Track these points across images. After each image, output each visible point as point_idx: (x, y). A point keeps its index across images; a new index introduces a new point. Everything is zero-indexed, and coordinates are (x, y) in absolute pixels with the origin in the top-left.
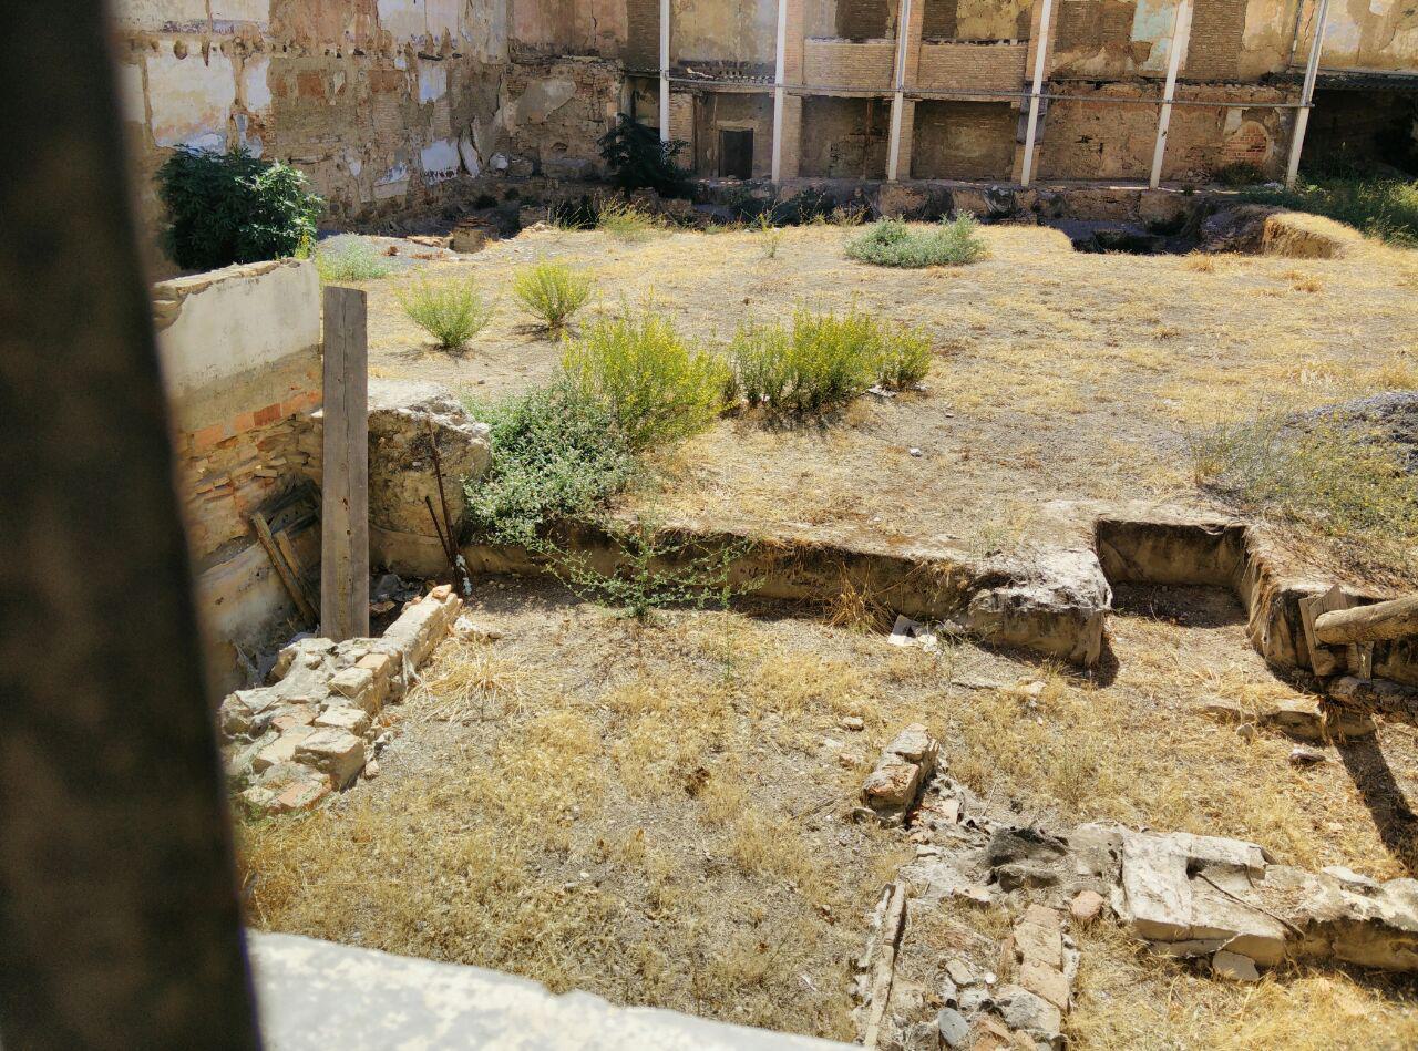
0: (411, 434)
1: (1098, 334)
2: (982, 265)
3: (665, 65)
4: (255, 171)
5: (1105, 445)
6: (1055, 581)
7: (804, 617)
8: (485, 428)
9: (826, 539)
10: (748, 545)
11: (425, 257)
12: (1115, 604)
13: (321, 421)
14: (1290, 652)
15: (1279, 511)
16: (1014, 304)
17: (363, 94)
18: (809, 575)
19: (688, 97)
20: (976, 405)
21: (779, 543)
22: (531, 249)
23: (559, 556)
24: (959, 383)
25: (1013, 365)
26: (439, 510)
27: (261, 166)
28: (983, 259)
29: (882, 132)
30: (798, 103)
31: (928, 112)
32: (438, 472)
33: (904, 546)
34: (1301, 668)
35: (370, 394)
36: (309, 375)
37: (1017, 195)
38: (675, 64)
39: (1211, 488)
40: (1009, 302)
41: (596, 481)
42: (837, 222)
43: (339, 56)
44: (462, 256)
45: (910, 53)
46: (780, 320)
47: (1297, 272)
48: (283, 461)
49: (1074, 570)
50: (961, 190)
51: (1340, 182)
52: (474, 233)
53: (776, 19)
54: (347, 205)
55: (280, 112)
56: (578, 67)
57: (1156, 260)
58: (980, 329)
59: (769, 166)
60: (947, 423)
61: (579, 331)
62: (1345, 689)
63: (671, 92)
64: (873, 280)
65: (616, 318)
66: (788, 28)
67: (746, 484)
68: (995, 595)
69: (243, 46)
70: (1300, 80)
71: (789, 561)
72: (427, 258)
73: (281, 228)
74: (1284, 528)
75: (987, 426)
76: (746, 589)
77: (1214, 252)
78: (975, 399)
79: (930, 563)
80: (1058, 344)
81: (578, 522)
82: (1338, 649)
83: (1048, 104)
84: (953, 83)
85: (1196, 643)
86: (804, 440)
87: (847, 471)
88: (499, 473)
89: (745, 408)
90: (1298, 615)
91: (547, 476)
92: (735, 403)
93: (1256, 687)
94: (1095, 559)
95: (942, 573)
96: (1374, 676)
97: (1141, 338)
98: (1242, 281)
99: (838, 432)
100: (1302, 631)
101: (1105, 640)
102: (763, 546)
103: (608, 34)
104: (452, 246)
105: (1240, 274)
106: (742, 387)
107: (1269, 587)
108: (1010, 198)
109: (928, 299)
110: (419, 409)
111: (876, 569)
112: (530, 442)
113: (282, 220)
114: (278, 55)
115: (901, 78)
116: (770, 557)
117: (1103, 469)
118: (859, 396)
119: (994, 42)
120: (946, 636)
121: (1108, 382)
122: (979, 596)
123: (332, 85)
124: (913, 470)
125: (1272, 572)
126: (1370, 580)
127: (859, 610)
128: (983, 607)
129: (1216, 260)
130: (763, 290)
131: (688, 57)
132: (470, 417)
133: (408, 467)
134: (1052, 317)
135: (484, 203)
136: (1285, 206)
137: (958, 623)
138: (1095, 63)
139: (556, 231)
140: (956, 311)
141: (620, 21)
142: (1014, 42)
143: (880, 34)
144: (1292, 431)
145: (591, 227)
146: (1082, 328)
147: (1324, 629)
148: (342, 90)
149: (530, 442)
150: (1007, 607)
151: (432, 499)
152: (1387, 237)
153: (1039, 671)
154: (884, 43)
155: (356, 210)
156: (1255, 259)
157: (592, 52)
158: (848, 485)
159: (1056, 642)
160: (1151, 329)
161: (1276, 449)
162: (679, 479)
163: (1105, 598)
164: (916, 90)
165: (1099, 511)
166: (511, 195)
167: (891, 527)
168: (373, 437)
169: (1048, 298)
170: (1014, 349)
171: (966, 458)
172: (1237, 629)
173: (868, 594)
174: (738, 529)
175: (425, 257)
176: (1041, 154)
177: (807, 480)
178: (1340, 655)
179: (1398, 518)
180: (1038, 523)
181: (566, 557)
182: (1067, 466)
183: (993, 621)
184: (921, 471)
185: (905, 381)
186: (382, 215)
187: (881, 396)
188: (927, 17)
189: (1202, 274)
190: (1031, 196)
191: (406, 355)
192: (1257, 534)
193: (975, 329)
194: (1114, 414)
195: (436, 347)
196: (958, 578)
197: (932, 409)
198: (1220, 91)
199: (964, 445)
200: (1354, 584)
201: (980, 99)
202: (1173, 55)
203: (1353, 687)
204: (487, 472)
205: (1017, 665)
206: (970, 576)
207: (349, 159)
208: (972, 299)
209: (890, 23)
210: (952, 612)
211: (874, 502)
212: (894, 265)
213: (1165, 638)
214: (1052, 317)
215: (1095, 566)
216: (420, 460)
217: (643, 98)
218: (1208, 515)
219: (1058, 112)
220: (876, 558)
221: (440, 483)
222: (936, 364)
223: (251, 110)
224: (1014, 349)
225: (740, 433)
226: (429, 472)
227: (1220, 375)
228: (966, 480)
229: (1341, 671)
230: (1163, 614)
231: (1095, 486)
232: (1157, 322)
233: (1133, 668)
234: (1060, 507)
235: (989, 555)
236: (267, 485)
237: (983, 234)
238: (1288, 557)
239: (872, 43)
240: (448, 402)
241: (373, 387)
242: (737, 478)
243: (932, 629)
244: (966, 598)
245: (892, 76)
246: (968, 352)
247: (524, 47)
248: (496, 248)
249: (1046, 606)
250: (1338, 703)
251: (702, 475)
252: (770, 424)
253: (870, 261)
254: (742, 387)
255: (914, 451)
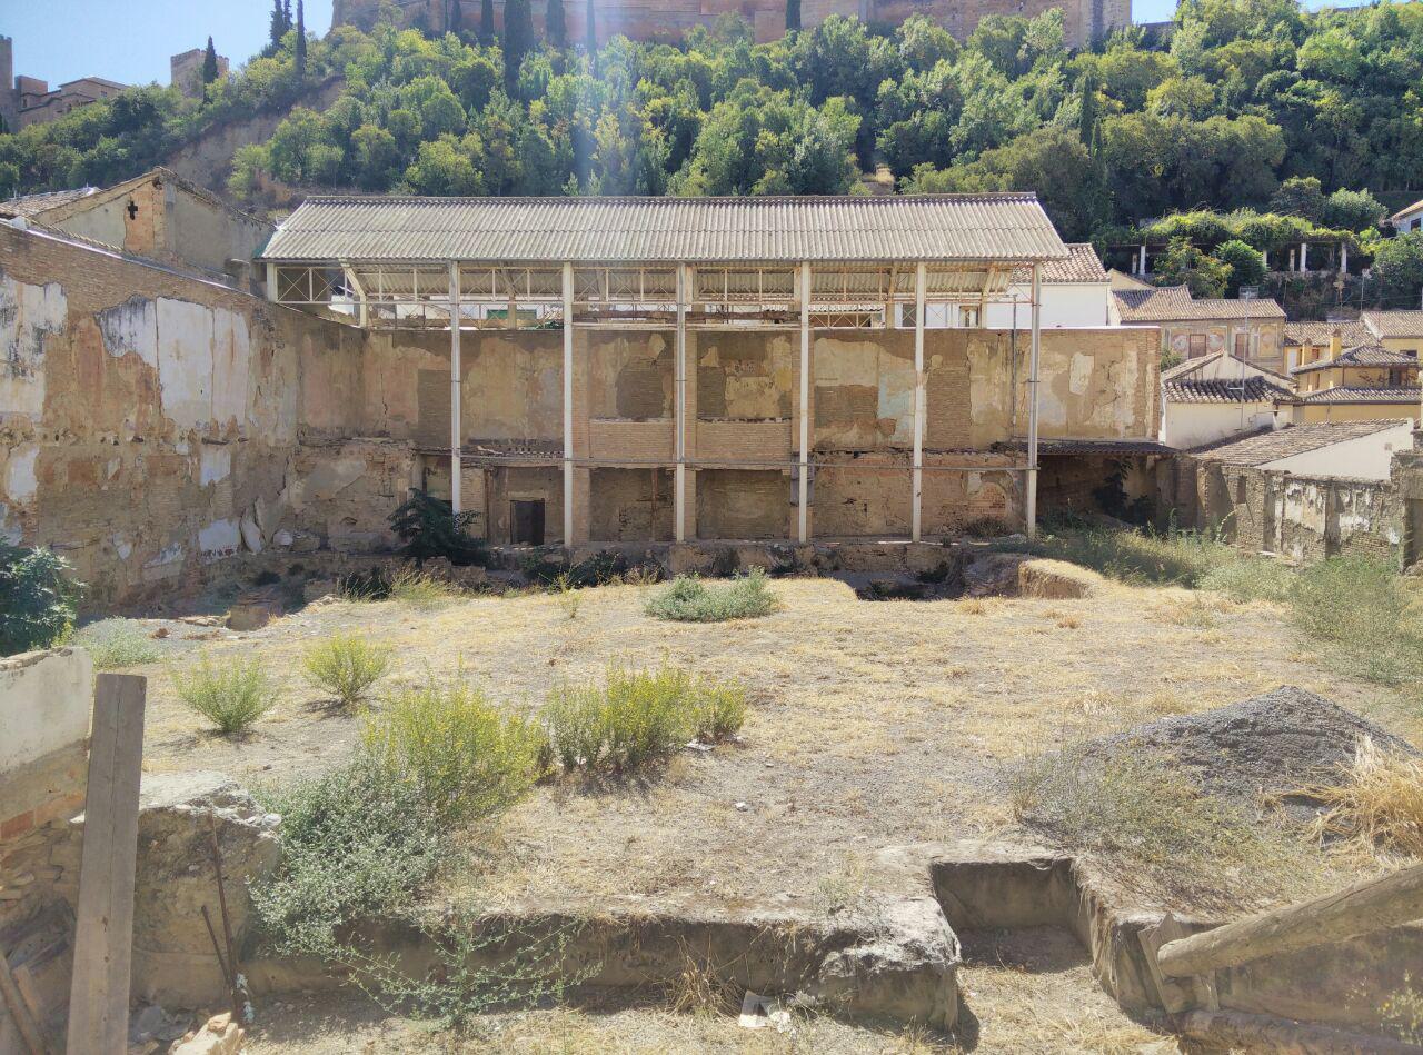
0: (189, 833)
1: (895, 675)
2: (776, 616)
3: (456, 443)
4: (11, 559)
5: (924, 786)
6: (903, 935)
7: (644, 1005)
8: (276, 818)
9: (662, 911)
10: (578, 926)
11: (198, 638)
12: (964, 955)
13: (81, 826)
14: (1140, 990)
15: (1099, 841)
16: (814, 652)
17: (140, 478)
18: (645, 954)
19: (480, 472)
20: (795, 753)
21: (612, 920)
22: (319, 622)
23: (362, 963)
24: (774, 732)
25: (823, 710)
26: (217, 920)
27: (18, 554)
28: (777, 610)
29: (667, 497)
30: (586, 474)
31: (709, 479)
32: (219, 875)
33: (744, 910)
34: (1152, 1006)
35: (142, 791)
36: (72, 775)
37: (797, 552)
38: (466, 443)
39: (1031, 822)
40: (808, 649)
41: (404, 869)
42: (633, 581)
43: (116, 443)
44: (242, 634)
45: (688, 429)
46: (590, 679)
47: (1057, 611)
48: (31, 878)
49: (919, 921)
50: (745, 547)
51: (1072, 531)
52: (254, 610)
53: (562, 401)
54: (112, 589)
55: (49, 501)
56: (369, 448)
57: (933, 605)
58: (785, 677)
59: (562, 532)
60: (768, 773)
61: (378, 704)
62: (1200, 1025)
63: (462, 467)
64: (676, 635)
65: (416, 688)
66: (574, 409)
67: (571, 858)
68: (845, 958)
69: (10, 435)
70: (1024, 448)
71: (624, 940)
72: (202, 638)
73: (35, 617)
74: (1107, 858)
75: (808, 774)
76: (580, 977)
77: (982, 596)
78: (792, 747)
79: (774, 926)
80: (860, 687)
81: (383, 918)
82: (1183, 982)
83: (815, 471)
84: (729, 455)
85: (1048, 991)
86: (626, 802)
87: (675, 831)
88: (290, 870)
89: (561, 774)
90: (1139, 949)
91: (347, 867)
92: (552, 769)
93: (1115, 1033)
94: (937, 907)
95: (787, 936)
96: (1222, 1007)
97: (935, 678)
98: (1011, 621)
99: (661, 791)
100: (1147, 966)
101: (960, 997)
102: (594, 925)
103: (397, 417)
104: (229, 624)
105: (1009, 614)
106: (557, 751)
107: (1107, 922)
108: (791, 553)
109: (732, 650)
110: (199, 803)
111: (718, 940)
112: (326, 830)
113: (39, 607)
114: (48, 445)
115: (681, 450)
116: (604, 938)
117: (927, 809)
118: (677, 752)
119: (762, 420)
120: (800, 1010)
121: (914, 722)
122: (829, 959)
123: (105, 472)
124: (742, 824)
125: (1106, 905)
126: (1197, 906)
127: (704, 989)
128: (834, 972)
129: (986, 603)
130: (568, 651)
131: (479, 436)
132: (259, 808)
133: (183, 872)
134: (851, 662)
135: (265, 579)
136: (1032, 554)
137: (810, 994)
138: (851, 437)
139: (347, 603)
140: (760, 660)
141: (412, 406)
142: (779, 420)
143: (658, 415)
144: (1092, 760)
145: (383, 596)
146: (880, 672)
147: (1168, 961)
148: (116, 476)
149: (326, 830)
150: (859, 969)
151: (209, 910)
152: (1123, 579)
153: (902, 1040)
154: (663, 421)
155: (122, 593)
156: (1017, 601)
157: (382, 434)
158: (678, 847)
159: (913, 1006)
160: (942, 669)
161: (1082, 778)
162: (496, 857)
163: (954, 950)
164: (695, 460)
165: (931, 854)
166: (296, 569)
167: (729, 890)
168: (143, 841)
169: (843, 644)
170: (820, 694)
171: (793, 809)
172: (1084, 970)
173: (711, 970)
174: (567, 908)
175: (198, 638)
176: (814, 514)
177: (634, 845)
178: (1188, 988)
179: (1207, 841)
180: (875, 872)
181: (371, 964)
182: (891, 810)
183: (846, 988)
184: (751, 826)
185: (721, 733)
186: (151, 597)
187: (699, 751)
188: (700, 400)
189: (974, 616)
190: (809, 553)
191: (178, 744)
192: (1084, 867)
193: (781, 677)
194: (926, 753)
195: (214, 733)
196: (805, 941)
197: (751, 759)
198: (961, 458)
199: (789, 796)
200: (1183, 911)
201: (754, 468)
202: (916, 430)
203: (1208, 1022)
204: (277, 869)
205: (878, 1036)
206: (817, 938)
207: (117, 543)
208: (772, 650)
209: (666, 404)
210: (802, 981)
211: (707, 863)
212: (693, 620)
213: (1016, 986)
214: (851, 662)
215: (939, 914)
216: (198, 863)
217: (434, 474)
218: (1033, 850)
219: (823, 477)
220: (717, 928)
221: (221, 889)
222: (750, 714)
223: (13, 498)
224: (820, 694)
225: (560, 801)
226: (208, 876)
227: (1013, 709)
228: (795, 832)
229: (1191, 1007)
230: (1010, 961)
231: (922, 827)
232: (945, 662)
233: (993, 1025)
234: (892, 852)
235: (832, 912)
236: (8, 909)
237: (773, 586)
238: (1118, 888)
239: (651, 422)
240: (234, 793)
241: (147, 783)
242: (560, 850)
243: (784, 1006)
244: (815, 963)
245: (673, 449)
246: (778, 700)
247: (313, 430)
248: (278, 624)
249: (898, 964)
250: (1194, 1040)
251: (522, 850)
252: (590, 788)
253: (670, 617)
254: (557, 751)
255: (740, 805)
